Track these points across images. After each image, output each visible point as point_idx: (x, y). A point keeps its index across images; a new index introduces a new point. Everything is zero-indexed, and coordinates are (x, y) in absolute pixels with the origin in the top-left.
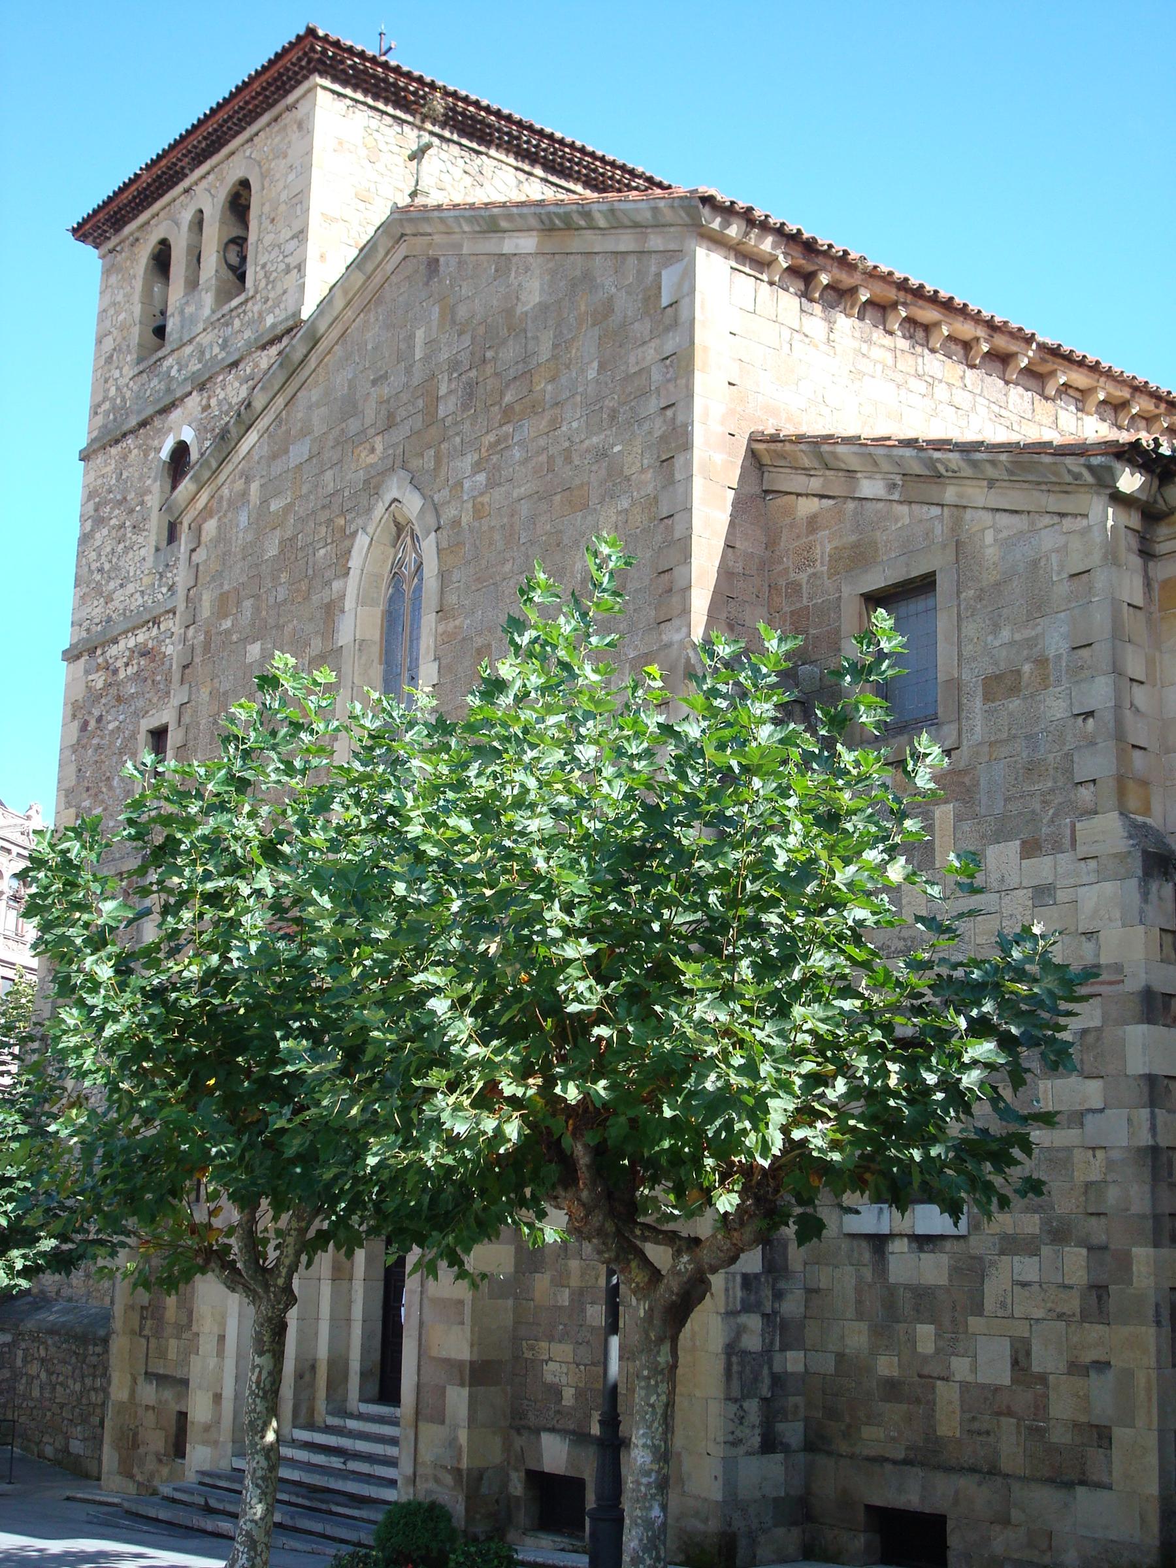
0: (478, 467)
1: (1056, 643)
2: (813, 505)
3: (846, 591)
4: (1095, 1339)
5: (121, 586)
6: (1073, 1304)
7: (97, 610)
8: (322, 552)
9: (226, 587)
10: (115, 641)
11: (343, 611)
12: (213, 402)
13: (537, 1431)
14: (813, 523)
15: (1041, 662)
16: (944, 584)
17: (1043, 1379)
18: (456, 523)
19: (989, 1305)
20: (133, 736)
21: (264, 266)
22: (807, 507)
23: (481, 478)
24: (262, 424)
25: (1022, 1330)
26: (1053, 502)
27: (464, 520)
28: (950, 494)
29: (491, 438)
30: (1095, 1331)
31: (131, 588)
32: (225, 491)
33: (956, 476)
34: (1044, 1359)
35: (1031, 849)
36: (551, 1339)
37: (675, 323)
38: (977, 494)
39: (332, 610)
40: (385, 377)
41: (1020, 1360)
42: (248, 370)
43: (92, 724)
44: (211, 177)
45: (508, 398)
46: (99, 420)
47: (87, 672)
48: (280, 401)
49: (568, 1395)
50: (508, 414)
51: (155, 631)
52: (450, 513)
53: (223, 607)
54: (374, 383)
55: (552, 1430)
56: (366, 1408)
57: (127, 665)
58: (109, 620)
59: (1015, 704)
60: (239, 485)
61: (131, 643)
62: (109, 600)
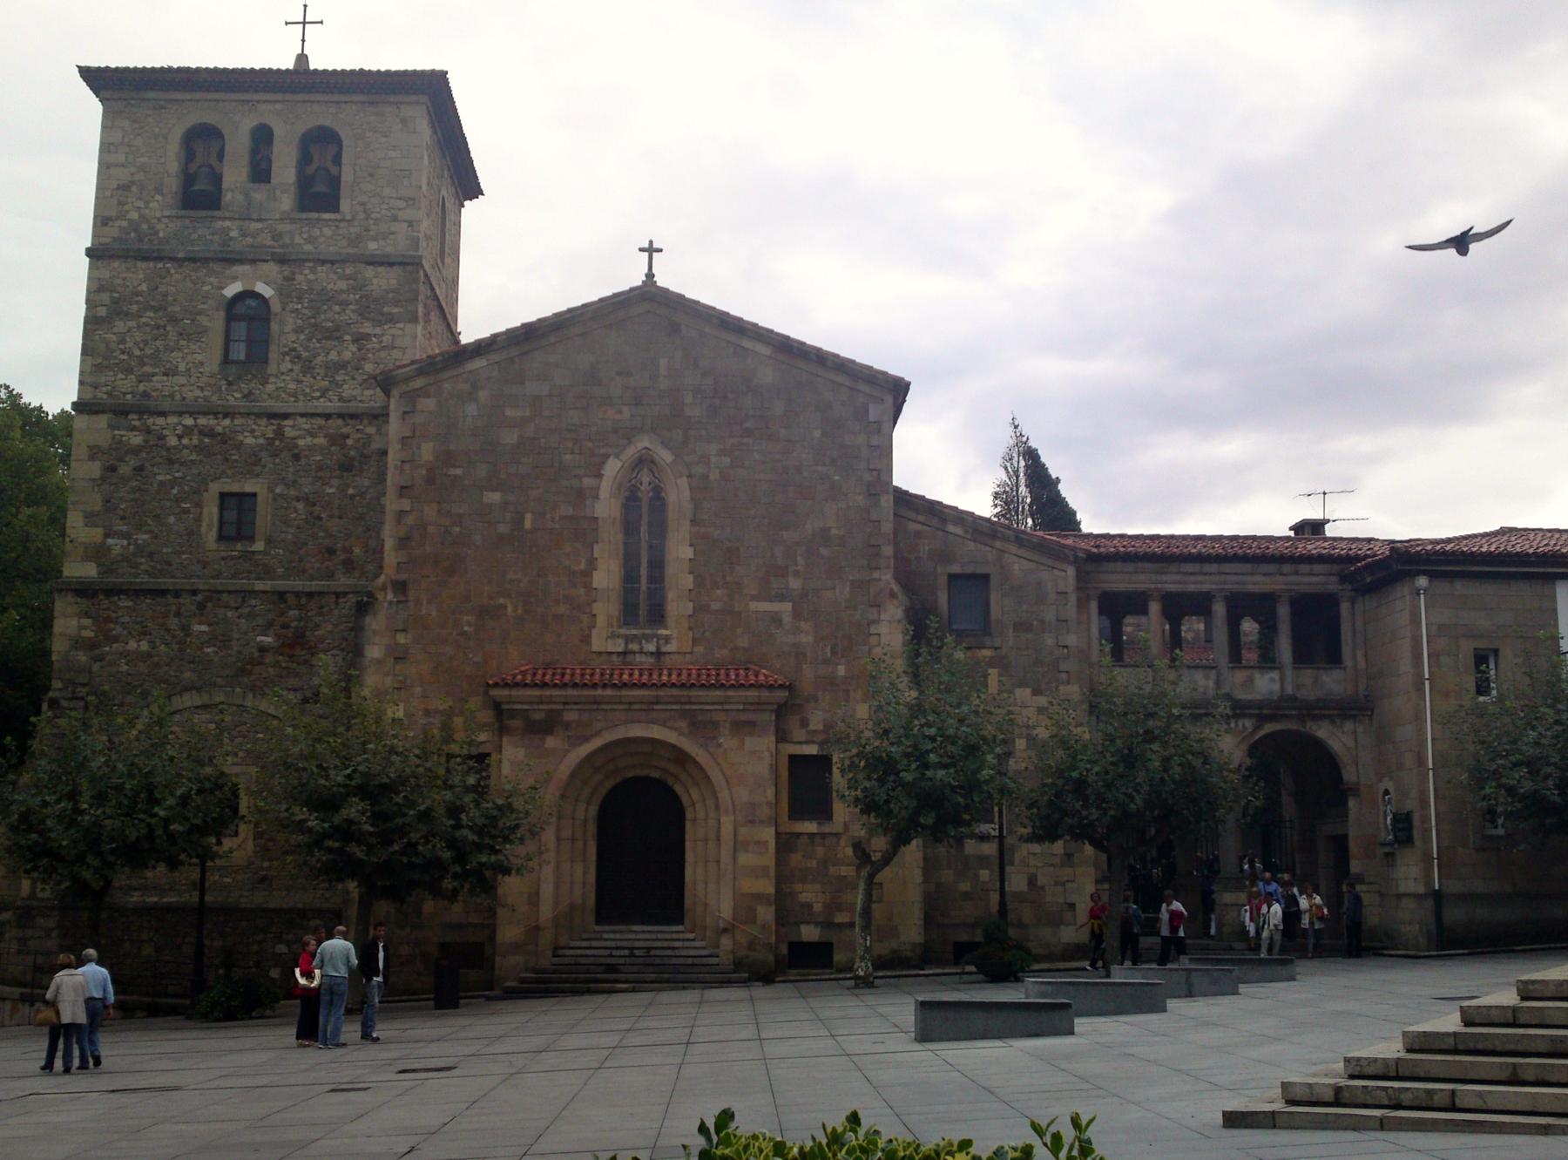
0: (722, 453)
1: (1050, 614)
2: (919, 527)
3: (939, 570)
4: (1066, 873)
5: (165, 374)
6: (1057, 861)
7: (125, 383)
8: (568, 457)
9: (452, 447)
10: (163, 414)
11: (597, 497)
12: (299, 277)
13: (797, 924)
14: (917, 534)
15: (1042, 622)
16: (994, 581)
17: (1043, 888)
18: (705, 477)
19: (1017, 861)
20: (197, 492)
21: (363, 204)
22: (913, 527)
23: (728, 460)
24: (496, 357)
25: (1033, 870)
26: (1050, 562)
27: (712, 477)
28: (998, 544)
29: (735, 441)
30: (1068, 870)
31: (183, 380)
32: (447, 386)
33: (1005, 539)
34: (1041, 881)
35: (1037, 692)
36: (803, 882)
37: (879, 431)
38: (1013, 549)
39: (580, 495)
40: (629, 374)
41: (1032, 881)
42: (348, 272)
43: (124, 469)
44: (278, 106)
45: (748, 425)
46: (113, 231)
47: (111, 427)
48: (514, 351)
49: (817, 907)
50: (748, 433)
51: (227, 422)
52: (699, 470)
53: (447, 458)
54: (619, 373)
55: (808, 923)
56: (598, 928)
57: (180, 437)
58: (146, 395)
59: (1029, 636)
60: (467, 387)
61: (189, 421)
62: (147, 377)
